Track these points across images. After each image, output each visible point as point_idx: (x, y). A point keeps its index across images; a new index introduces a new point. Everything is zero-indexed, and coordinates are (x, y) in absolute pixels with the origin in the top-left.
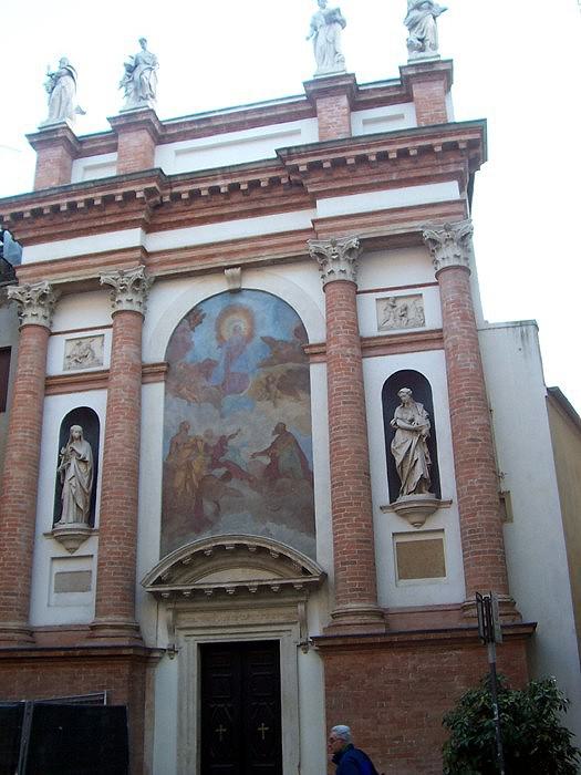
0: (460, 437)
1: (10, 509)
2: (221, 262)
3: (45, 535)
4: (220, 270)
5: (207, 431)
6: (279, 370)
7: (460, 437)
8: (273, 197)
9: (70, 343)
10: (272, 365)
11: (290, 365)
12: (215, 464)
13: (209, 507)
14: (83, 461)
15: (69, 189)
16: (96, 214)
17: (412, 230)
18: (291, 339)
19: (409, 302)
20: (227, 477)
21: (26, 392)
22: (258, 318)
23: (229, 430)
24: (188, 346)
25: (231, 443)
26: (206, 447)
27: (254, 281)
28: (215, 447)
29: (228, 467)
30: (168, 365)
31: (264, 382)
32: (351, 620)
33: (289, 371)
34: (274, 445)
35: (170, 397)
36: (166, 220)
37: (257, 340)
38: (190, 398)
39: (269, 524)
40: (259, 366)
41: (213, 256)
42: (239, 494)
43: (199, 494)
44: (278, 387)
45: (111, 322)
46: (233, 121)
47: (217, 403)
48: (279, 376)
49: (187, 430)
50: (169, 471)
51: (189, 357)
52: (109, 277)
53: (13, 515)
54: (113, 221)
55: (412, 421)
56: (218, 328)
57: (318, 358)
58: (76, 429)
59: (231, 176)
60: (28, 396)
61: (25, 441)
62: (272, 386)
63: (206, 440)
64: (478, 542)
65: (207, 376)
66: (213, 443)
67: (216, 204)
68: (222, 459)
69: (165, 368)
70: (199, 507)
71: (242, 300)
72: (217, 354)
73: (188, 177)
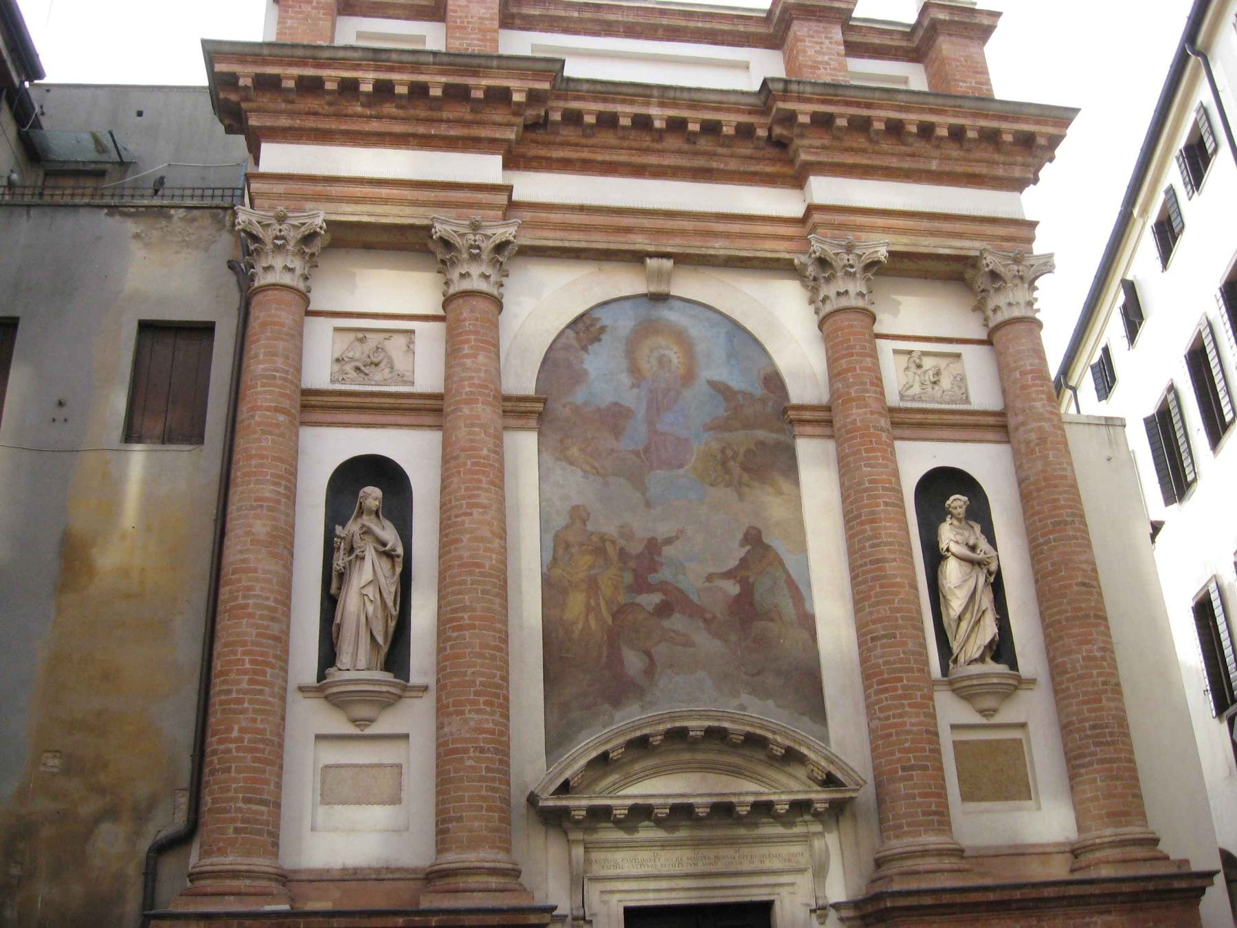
1: (254, 631)
2: (640, 243)
3: (302, 689)
4: (637, 258)
5: (622, 527)
6: (741, 439)
8: (731, 156)
9: (339, 335)
10: (730, 429)
11: (761, 434)
12: (640, 586)
13: (633, 662)
14: (390, 555)
15: (383, 56)
16: (423, 113)
17: (963, 253)
18: (759, 391)
19: (942, 363)
20: (664, 610)
21: (277, 410)
22: (700, 348)
23: (663, 530)
24: (578, 377)
25: (668, 551)
26: (622, 553)
27: (690, 286)
28: (638, 557)
29: (665, 593)
30: (545, 401)
31: (719, 456)
32: (931, 863)
33: (761, 444)
34: (744, 562)
35: (547, 457)
36: (543, 152)
37: (700, 386)
38: (587, 468)
39: (745, 698)
40: (708, 428)
41: (628, 230)
42: (688, 643)
43: (614, 638)
44: (745, 468)
45: (441, 312)
46: (641, 20)
47: (637, 479)
48: (742, 450)
49: (584, 522)
50: (552, 589)
51: (580, 396)
52: (449, 228)
53: (259, 644)
54: (452, 133)
55: (973, 548)
56: (631, 352)
57: (808, 429)
58: (372, 495)
59: (674, 104)
60: (281, 418)
61: (278, 502)
62: (732, 464)
63: (622, 543)
65: (617, 432)
66: (636, 548)
67: (635, 144)
68: (653, 578)
69: (539, 407)
70: (615, 660)
71: (670, 314)
72: (630, 398)
73: (599, 88)
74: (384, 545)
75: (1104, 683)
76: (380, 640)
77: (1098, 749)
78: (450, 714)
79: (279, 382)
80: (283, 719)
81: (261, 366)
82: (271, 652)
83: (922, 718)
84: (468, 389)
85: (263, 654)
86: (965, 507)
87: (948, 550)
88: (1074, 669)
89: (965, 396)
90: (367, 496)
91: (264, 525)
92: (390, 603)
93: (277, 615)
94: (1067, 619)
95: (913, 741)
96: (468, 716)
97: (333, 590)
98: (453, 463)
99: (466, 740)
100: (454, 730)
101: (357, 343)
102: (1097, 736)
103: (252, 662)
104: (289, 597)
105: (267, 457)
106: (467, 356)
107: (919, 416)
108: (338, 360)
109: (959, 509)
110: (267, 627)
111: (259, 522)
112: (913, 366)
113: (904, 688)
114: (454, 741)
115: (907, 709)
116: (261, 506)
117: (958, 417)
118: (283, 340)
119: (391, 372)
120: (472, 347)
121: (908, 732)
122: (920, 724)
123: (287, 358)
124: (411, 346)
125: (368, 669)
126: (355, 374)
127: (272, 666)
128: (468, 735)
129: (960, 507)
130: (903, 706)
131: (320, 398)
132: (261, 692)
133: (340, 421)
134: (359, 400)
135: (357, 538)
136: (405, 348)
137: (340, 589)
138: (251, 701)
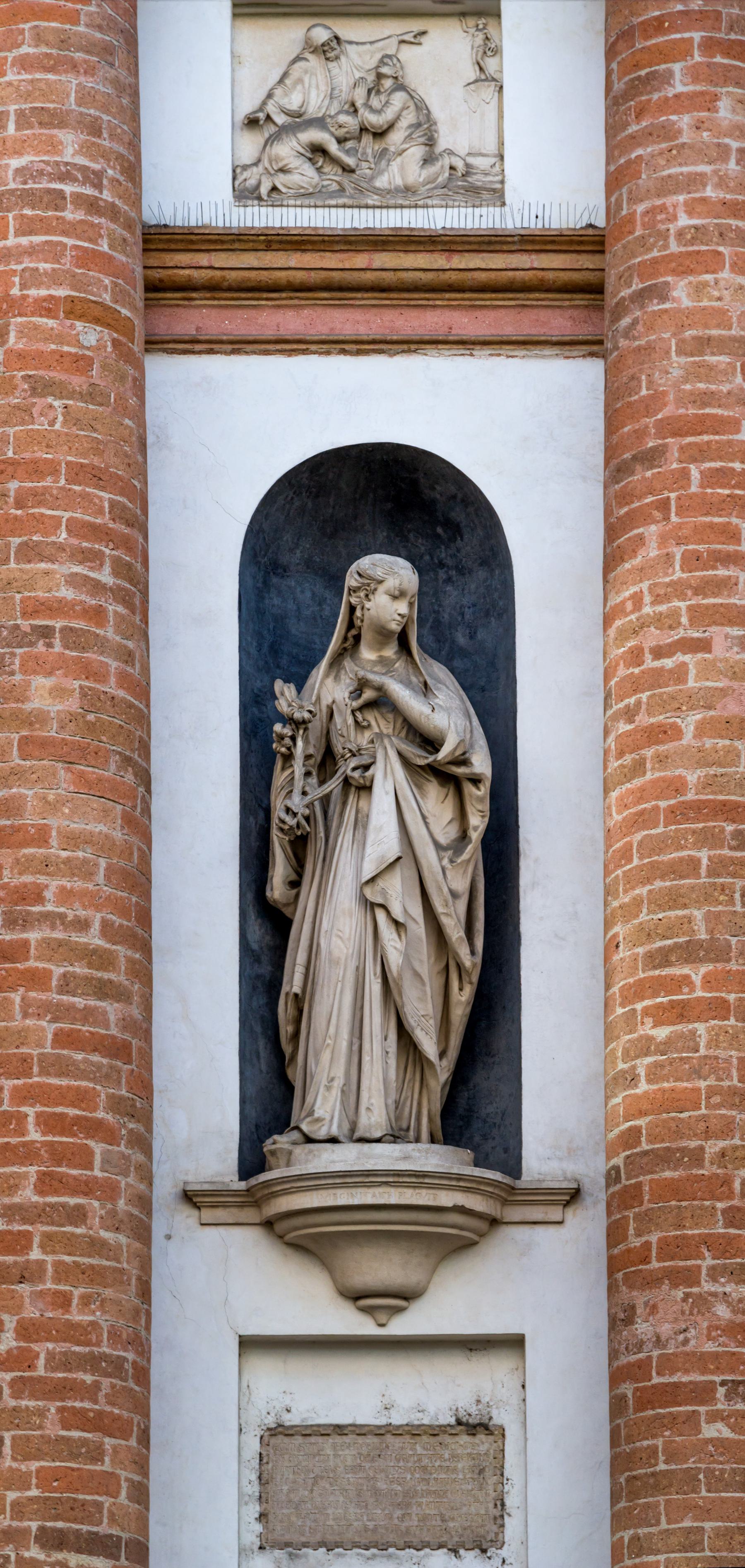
1: (50, 1029)
53: (63, 1068)
61: (97, 615)
74: (431, 743)
76: (429, 1046)
78: (652, 1281)
79: (71, 214)
80: (145, 1293)
81: (15, 163)
82: (103, 1092)
84: (684, 221)
85: (82, 1098)
90: (369, 586)
91: (58, 692)
92: (455, 931)
93: (118, 976)
96: (707, 1286)
97: (277, 890)
98: (644, 474)
99: (702, 1361)
100: (666, 1329)
101: (314, 62)
103: (48, 1123)
104: (145, 918)
105: (53, 469)
106: (681, 103)
108: (252, 123)
110: (87, 1015)
111: (41, 683)
114: (667, 1364)
116: (46, 633)
118: (74, 67)
119: (428, 160)
120: (694, 74)
123: (95, 129)
124: (491, 64)
125: (395, 1136)
126: (309, 170)
127: (109, 1135)
128: (710, 1347)
131: (203, 259)
132: (78, 1215)
133: (269, 333)
134: (331, 260)
135: (343, 721)
136: (472, 73)
137: (295, 884)
138: (49, 1243)
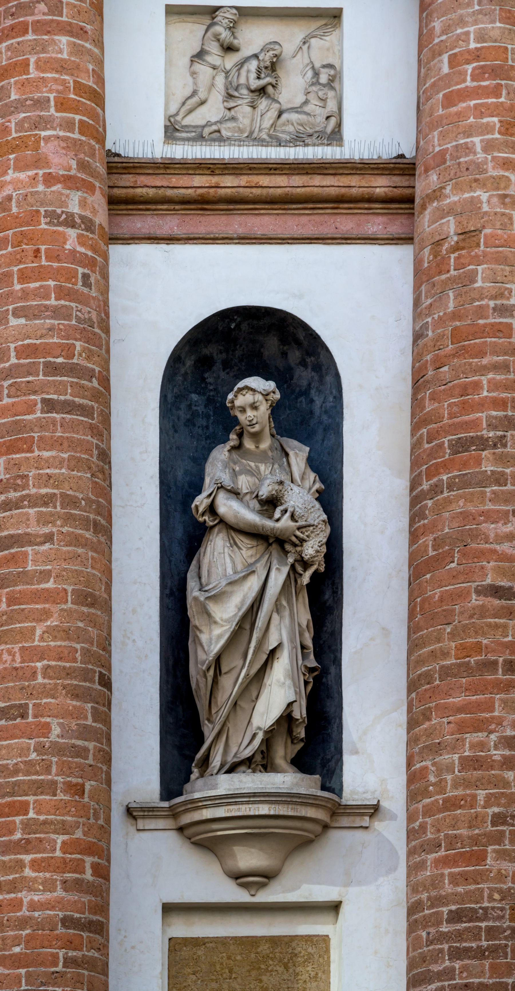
0: (454, 576)
7: (454, 576)
64: (480, 954)
75: (498, 819)
77: (457, 965)
83: (60, 893)
86: (264, 409)
87: (212, 509)
88: (440, 786)
89: (333, 121)
94: (446, 672)
95: (29, 940)
102: (459, 935)
107: (198, 180)
109: (250, 413)
112: (214, 48)
113: (27, 826)
115: (28, 872)
117: (297, 180)
121: (23, 923)
122: (58, 904)
129: (254, 407)
130: (21, 865)
